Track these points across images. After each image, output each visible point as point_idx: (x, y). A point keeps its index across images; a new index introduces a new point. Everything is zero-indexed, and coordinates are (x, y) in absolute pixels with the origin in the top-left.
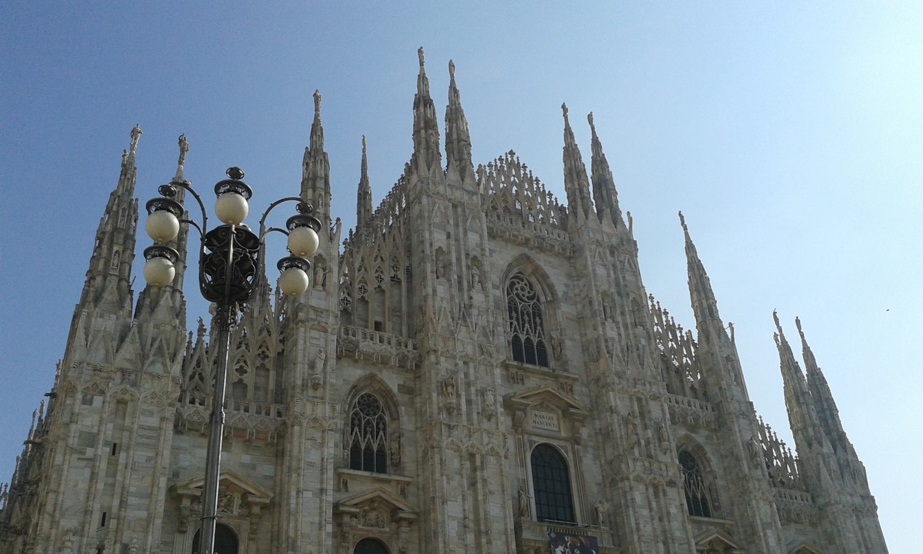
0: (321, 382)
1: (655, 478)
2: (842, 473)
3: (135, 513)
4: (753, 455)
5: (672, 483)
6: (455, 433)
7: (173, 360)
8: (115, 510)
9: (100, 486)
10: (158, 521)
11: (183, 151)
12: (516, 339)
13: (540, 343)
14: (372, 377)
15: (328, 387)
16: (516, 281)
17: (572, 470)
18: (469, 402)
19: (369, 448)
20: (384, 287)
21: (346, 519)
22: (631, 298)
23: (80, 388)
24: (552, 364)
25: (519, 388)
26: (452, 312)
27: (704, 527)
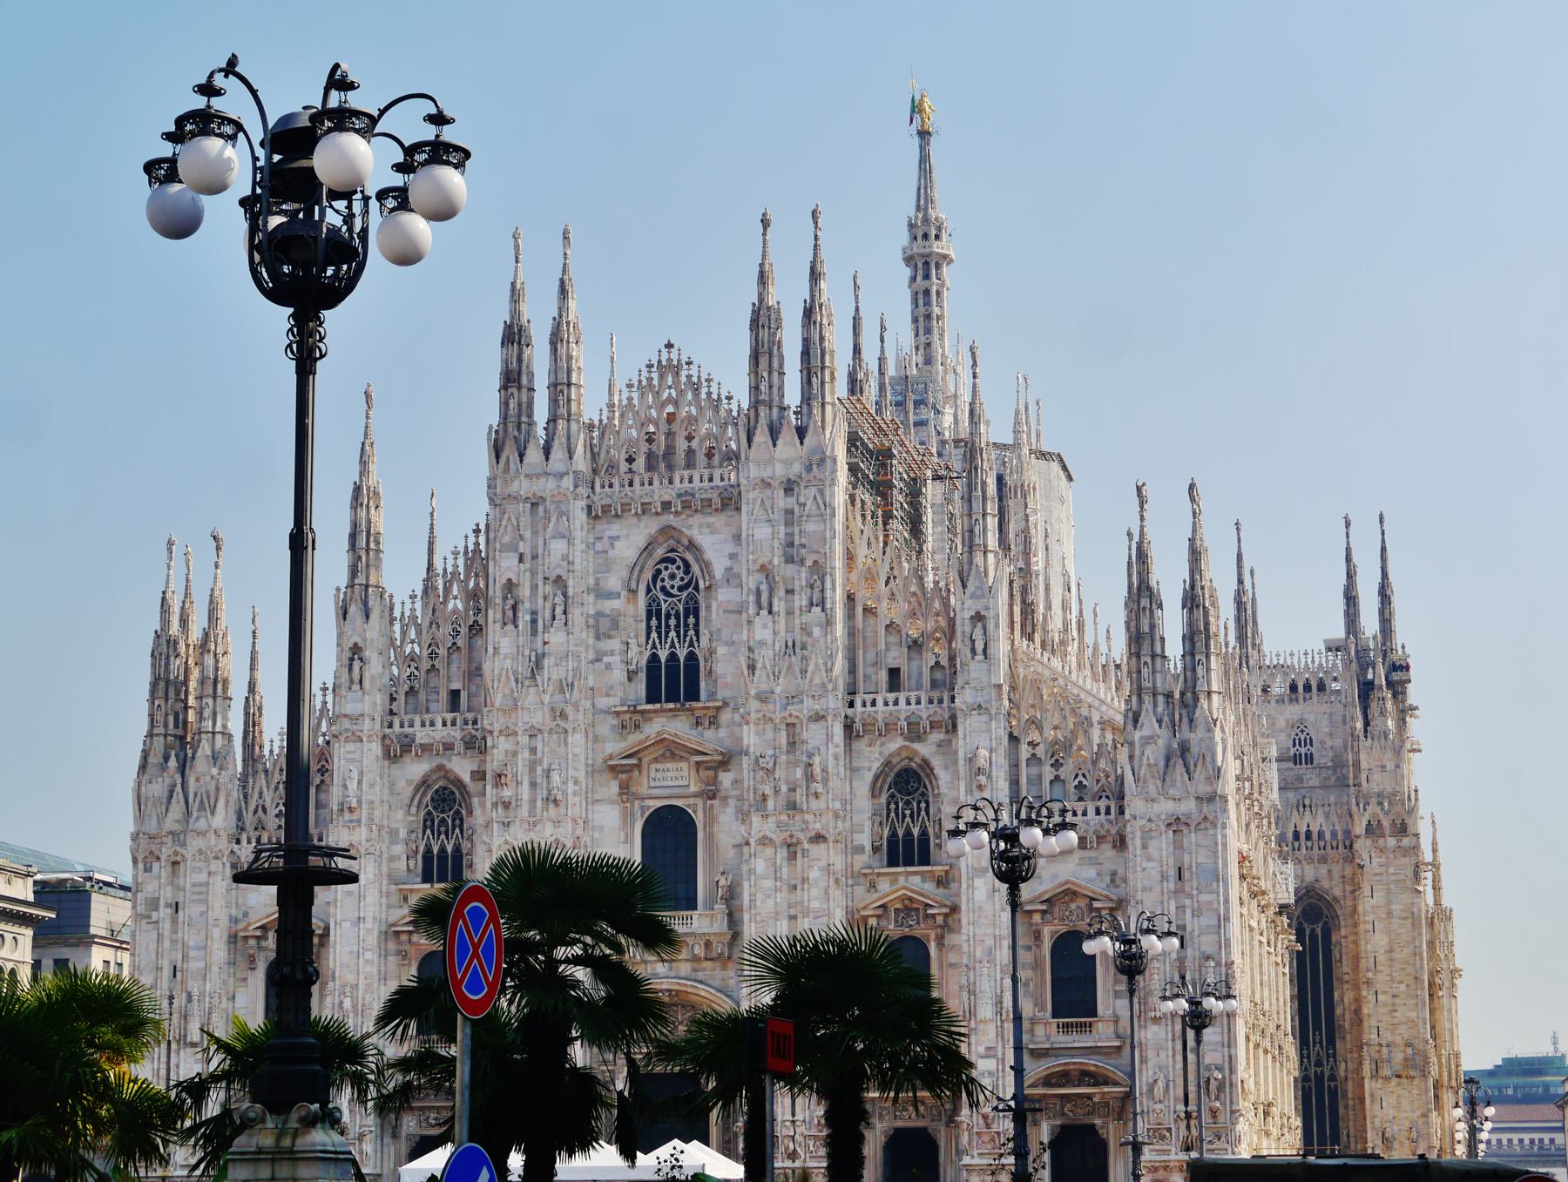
0: (354, 804)
1: (791, 836)
2: (1167, 766)
3: (195, 965)
4: (979, 771)
5: (819, 838)
6: (512, 829)
7: (213, 813)
8: (179, 965)
9: (167, 944)
10: (215, 969)
11: (218, 548)
12: (654, 658)
13: (691, 657)
14: (441, 767)
15: (365, 806)
16: (662, 566)
17: (700, 835)
18: (533, 785)
19: (443, 850)
20: (460, 642)
21: (404, 937)
22: (809, 563)
23: (140, 859)
24: (702, 684)
25: (634, 738)
26: (515, 673)
27: (902, 879)
